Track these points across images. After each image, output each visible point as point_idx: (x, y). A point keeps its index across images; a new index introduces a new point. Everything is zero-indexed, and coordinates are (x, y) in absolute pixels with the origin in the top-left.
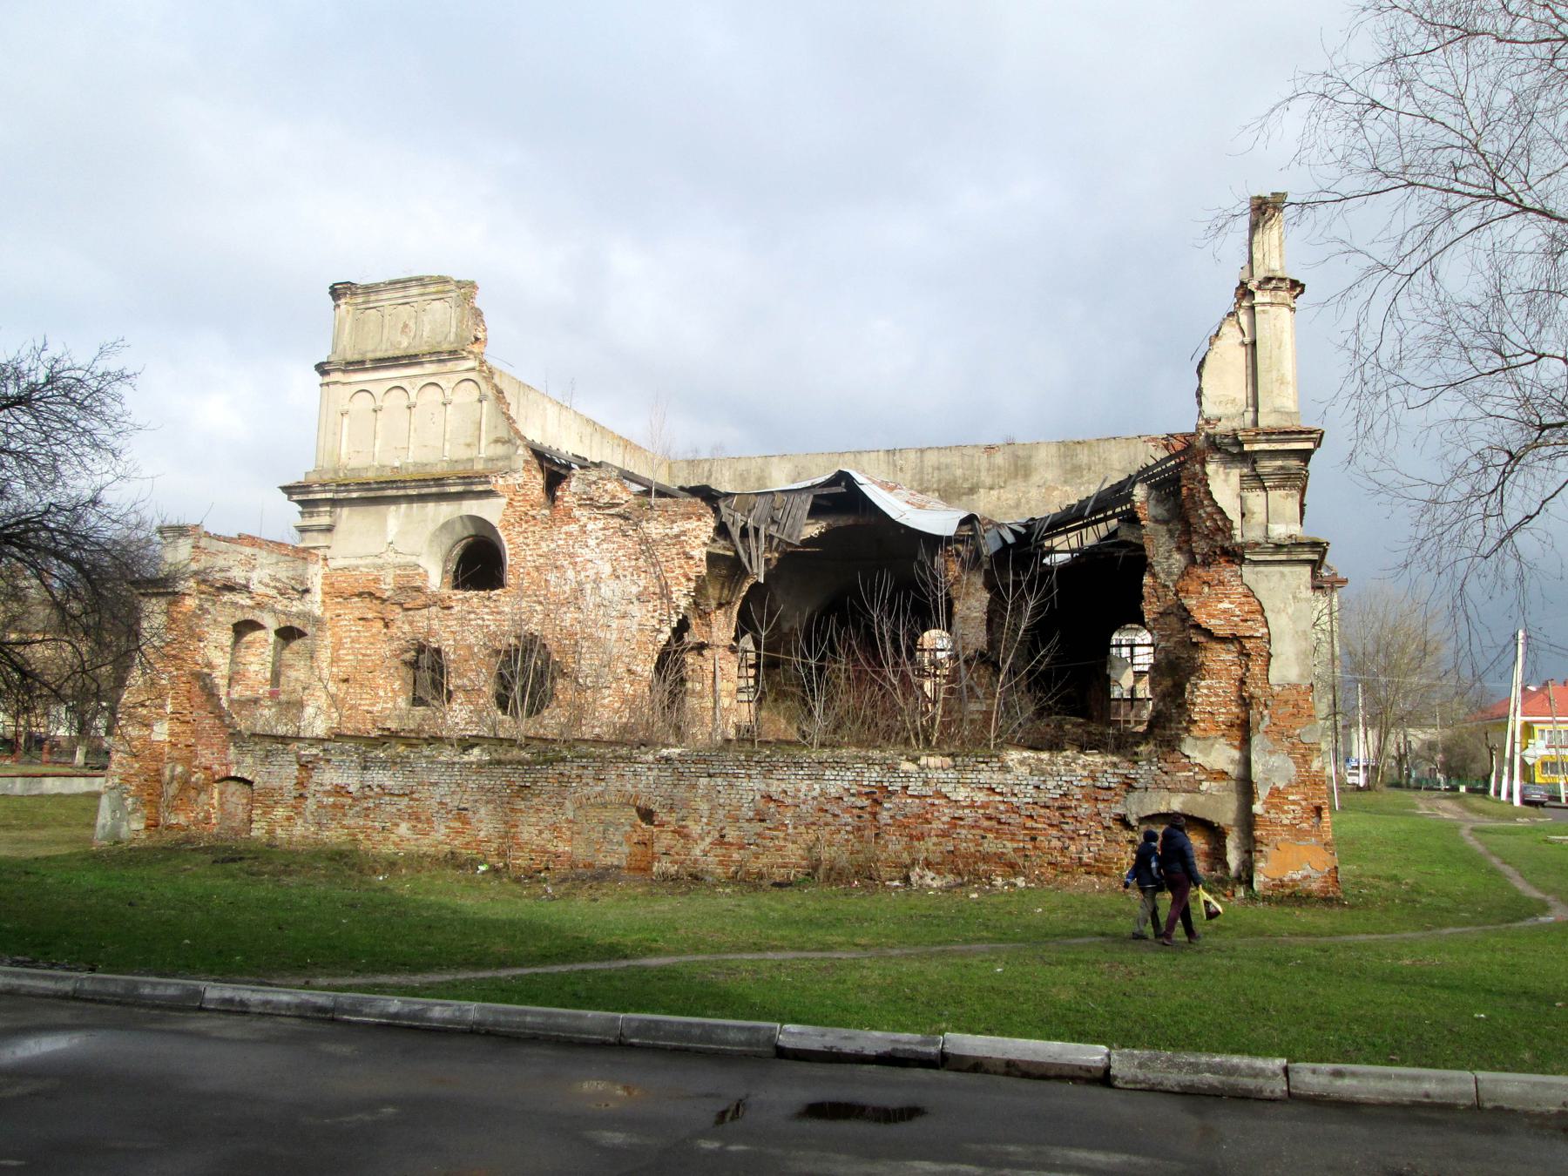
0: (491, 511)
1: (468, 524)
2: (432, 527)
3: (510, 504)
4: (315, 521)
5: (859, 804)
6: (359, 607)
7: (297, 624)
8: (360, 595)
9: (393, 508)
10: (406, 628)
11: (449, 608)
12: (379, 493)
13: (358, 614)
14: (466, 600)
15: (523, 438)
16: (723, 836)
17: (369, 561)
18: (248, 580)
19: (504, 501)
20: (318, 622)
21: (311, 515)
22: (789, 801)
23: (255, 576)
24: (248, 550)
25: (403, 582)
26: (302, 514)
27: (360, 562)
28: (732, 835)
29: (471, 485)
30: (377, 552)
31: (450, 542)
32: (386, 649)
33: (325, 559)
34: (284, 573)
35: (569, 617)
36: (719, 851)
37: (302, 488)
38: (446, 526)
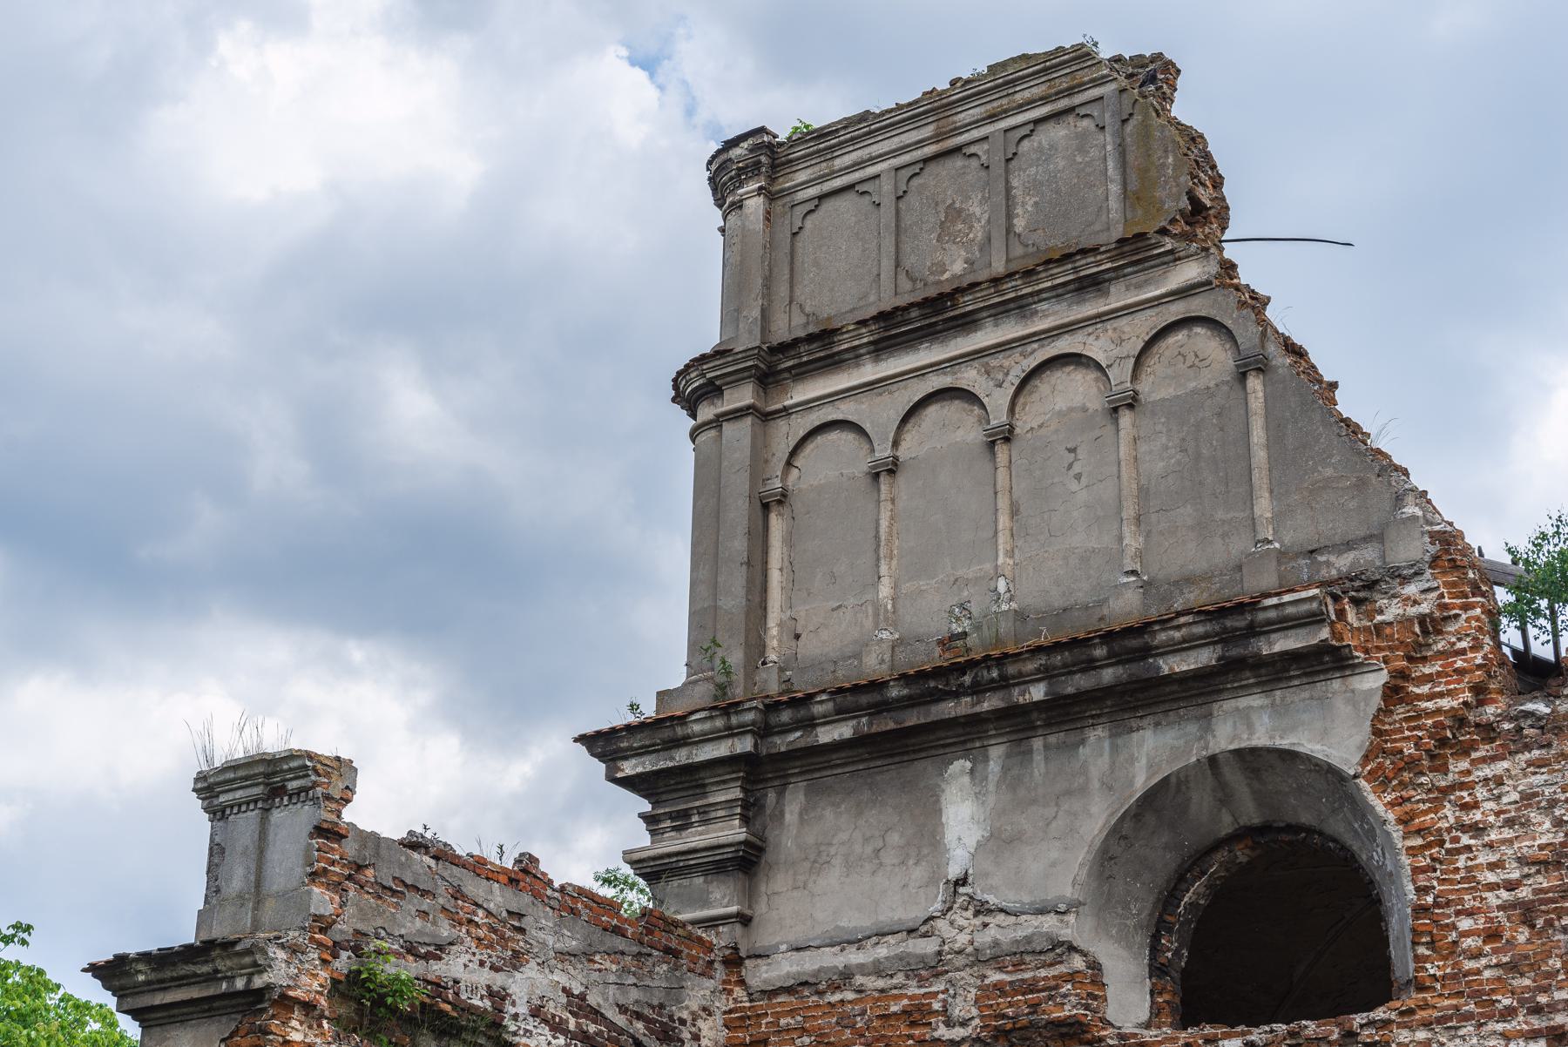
1: (1234, 776)
2: (1096, 818)
3: (1394, 693)
4: (697, 838)
9: (961, 765)
12: (913, 718)
17: (882, 952)
18: (499, 997)
19: (1374, 681)
21: (682, 821)
24: (498, 898)
25: (1015, 1007)
26: (649, 819)
27: (854, 957)
29: (1243, 646)
30: (913, 914)
31: (1165, 861)
33: (734, 961)
37: (661, 730)
38: (1158, 802)
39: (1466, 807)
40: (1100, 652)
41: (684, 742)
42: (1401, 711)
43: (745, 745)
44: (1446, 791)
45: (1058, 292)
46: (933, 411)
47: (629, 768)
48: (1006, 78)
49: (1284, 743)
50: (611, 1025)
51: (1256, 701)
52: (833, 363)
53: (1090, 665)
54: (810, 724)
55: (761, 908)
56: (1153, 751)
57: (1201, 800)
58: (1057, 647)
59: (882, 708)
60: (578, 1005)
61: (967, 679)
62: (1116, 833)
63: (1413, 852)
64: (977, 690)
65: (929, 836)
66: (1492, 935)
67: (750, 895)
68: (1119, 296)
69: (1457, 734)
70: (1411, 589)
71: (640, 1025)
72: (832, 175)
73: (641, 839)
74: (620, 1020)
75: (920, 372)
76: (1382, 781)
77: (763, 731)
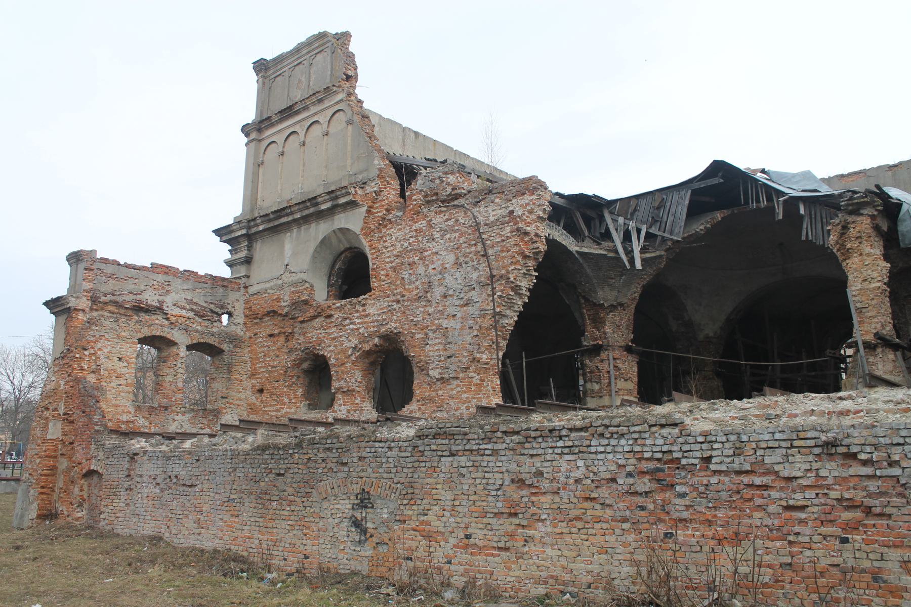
0: (353, 221)
2: (312, 246)
3: (369, 212)
5: (640, 488)
6: (269, 326)
7: (211, 340)
8: (268, 313)
10: (302, 339)
11: (330, 316)
12: (276, 223)
13: (268, 331)
14: (341, 308)
15: (380, 150)
16: (468, 537)
17: (272, 284)
18: (161, 302)
20: (235, 340)
22: (545, 485)
23: (169, 300)
24: (161, 278)
27: (268, 285)
28: (479, 537)
29: (336, 201)
30: (278, 275)
31: (330, 258)
32: (286, 360)
33: (246, 287)
34: (201, 298)
35: (419, 312)
36: (466, 557)
38: (324, 242)
39: (385, 242)
40: (308, 204)
41: (232, 232)
42: (371, 217)
43: (244, 232)
44: (381, 237)
45: (313, 104)
46: (291, 137)
47: (225, 238)
48: (309, 43)
49: (346, 226)
50: (202, 306)
51: (342, 215)
52: (272, 125)
53: (307, 208)
54: (257, 225)
55: (252, 275)
56: (320, 230)
57: (334, 241)
58: (299, 203)
59: (270, 221)
60: (190, 302)
61: (284, 212)
62: (315, 251)
63: (372, 254)
64: (287, 215)
65: (282, 253)
66: (387, 275)
67: (249, 270)
68: (327, 103)
69: (384, 222)
70: (373, 184)
71: (212, 306)
72: (277, 71)
73: (228, 256)
74: (205, 305)
75: (288, 127)
76: (366, 235)
77: (249, 228)
